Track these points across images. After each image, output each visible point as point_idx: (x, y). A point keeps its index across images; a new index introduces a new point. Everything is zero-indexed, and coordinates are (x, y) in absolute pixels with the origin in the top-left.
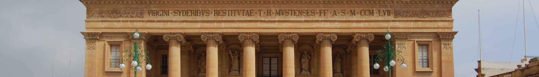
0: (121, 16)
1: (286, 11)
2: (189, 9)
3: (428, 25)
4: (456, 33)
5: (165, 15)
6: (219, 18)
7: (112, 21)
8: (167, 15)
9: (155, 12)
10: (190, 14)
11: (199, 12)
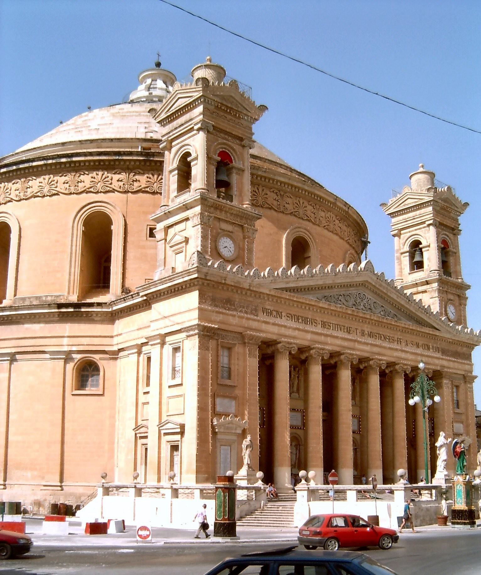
0: (235, 310)
1: (376, 334)
2: (300, 315)
3: (460, 367)
4: (476, 377)
5: (279, 317)
6: (325, 331)
7: (227, 315)
8: (280, 317)
9: (269, 311)
10: (300, 320)
11: (308, 319)
